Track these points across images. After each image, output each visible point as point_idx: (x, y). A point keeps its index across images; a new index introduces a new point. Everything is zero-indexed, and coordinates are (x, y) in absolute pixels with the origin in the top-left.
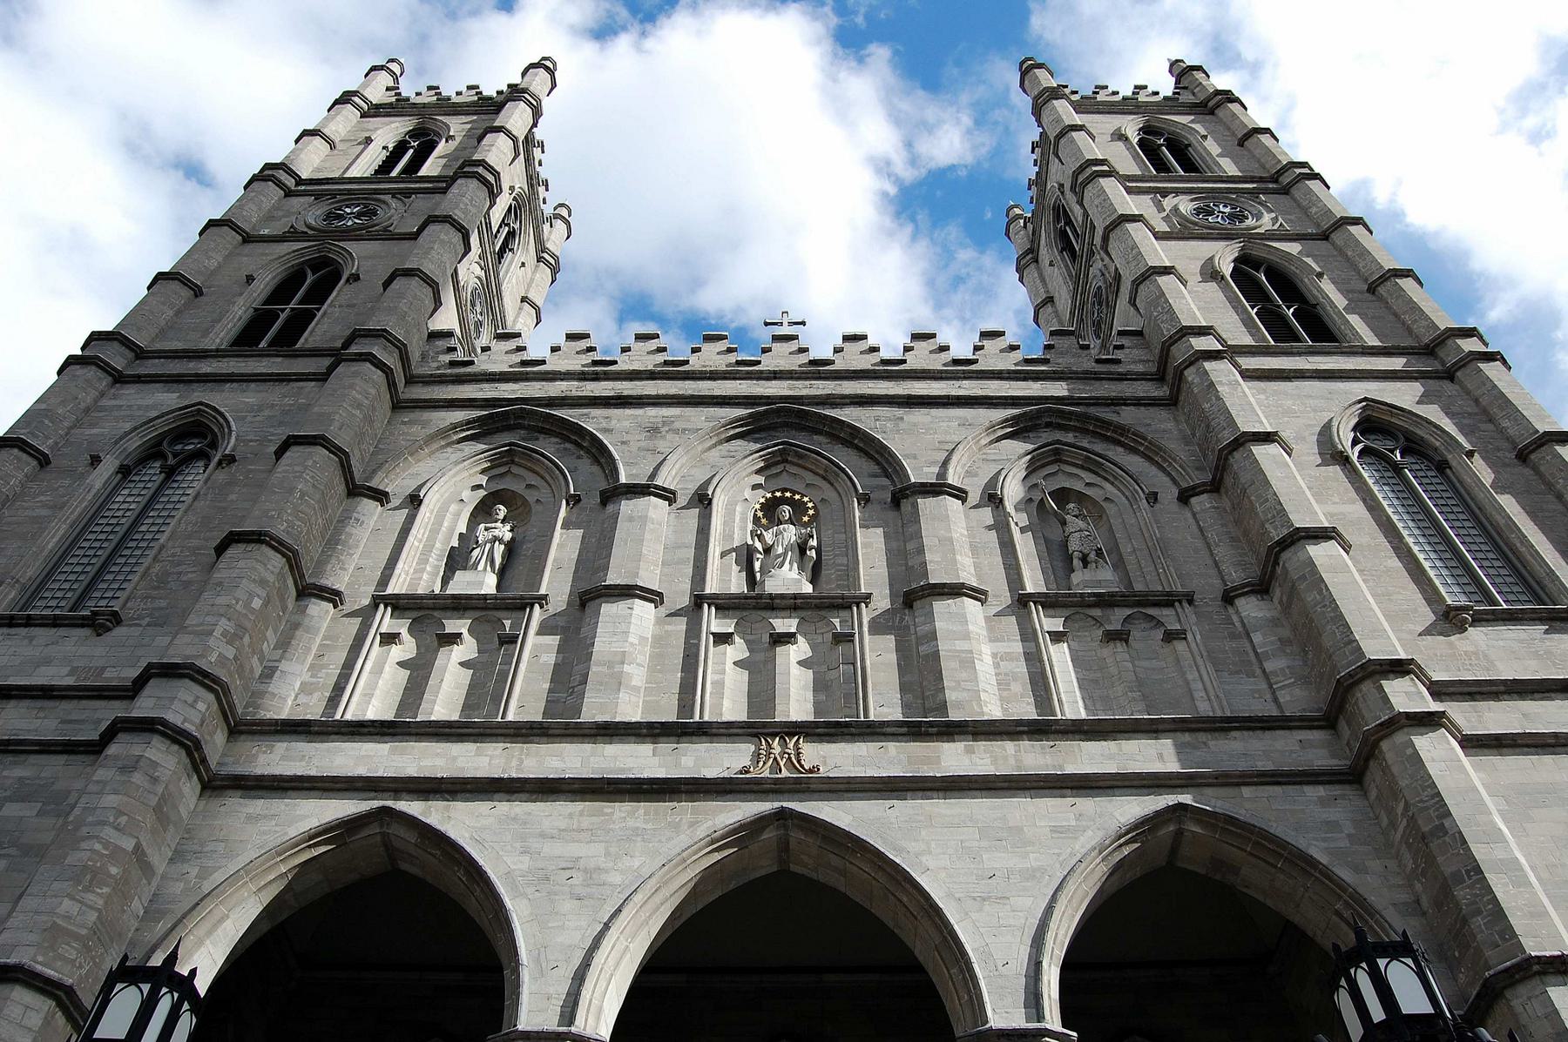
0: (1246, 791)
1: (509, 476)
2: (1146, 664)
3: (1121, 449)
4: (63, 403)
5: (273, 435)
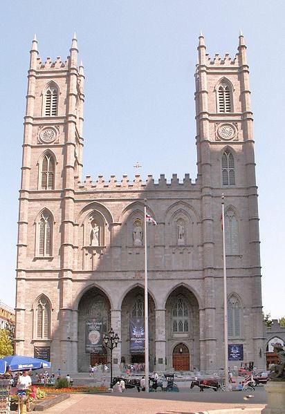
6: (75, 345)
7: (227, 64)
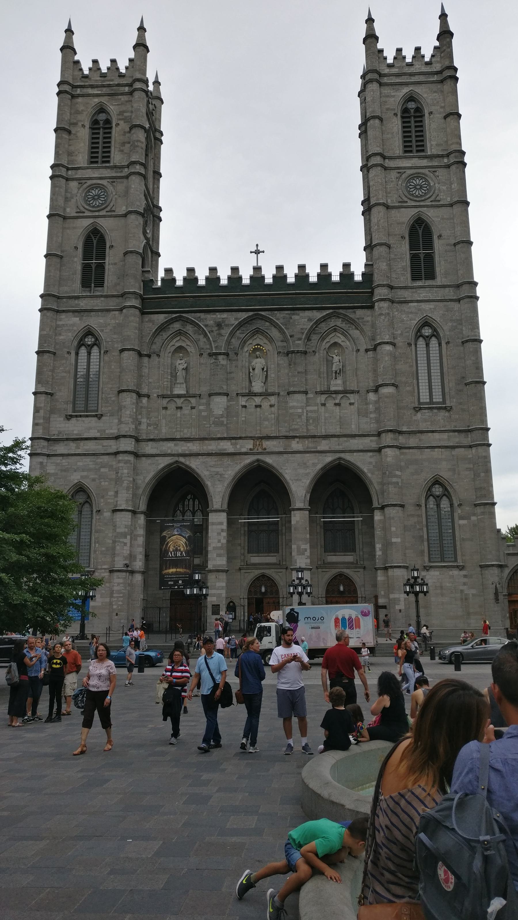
0: (355, 454)
1: (181, 341)
2: (343, 411)
3: (354, 327)
4: (50, 330)
5: (115, 339)
6: (138, 578)
7: (418, 67)
